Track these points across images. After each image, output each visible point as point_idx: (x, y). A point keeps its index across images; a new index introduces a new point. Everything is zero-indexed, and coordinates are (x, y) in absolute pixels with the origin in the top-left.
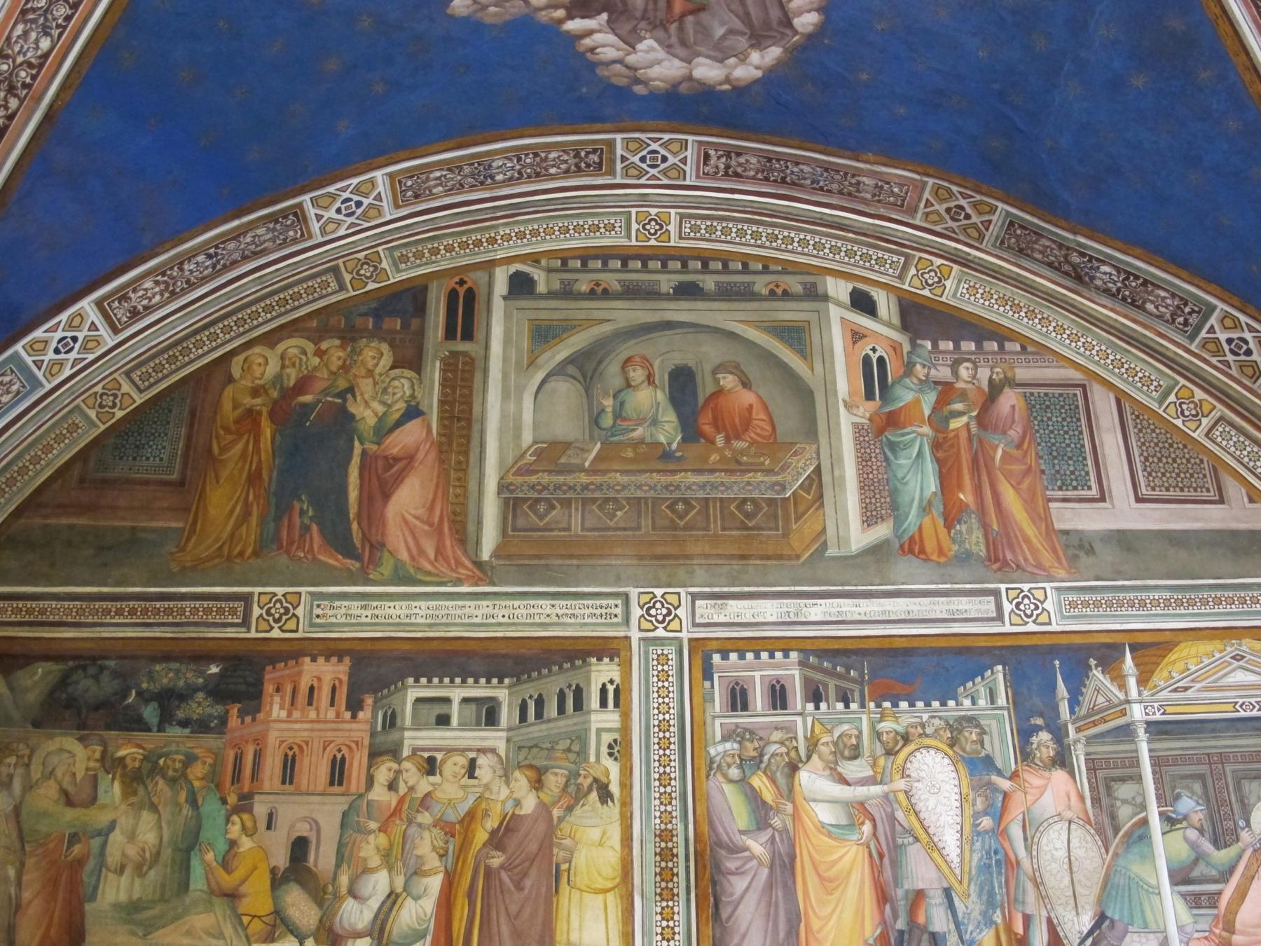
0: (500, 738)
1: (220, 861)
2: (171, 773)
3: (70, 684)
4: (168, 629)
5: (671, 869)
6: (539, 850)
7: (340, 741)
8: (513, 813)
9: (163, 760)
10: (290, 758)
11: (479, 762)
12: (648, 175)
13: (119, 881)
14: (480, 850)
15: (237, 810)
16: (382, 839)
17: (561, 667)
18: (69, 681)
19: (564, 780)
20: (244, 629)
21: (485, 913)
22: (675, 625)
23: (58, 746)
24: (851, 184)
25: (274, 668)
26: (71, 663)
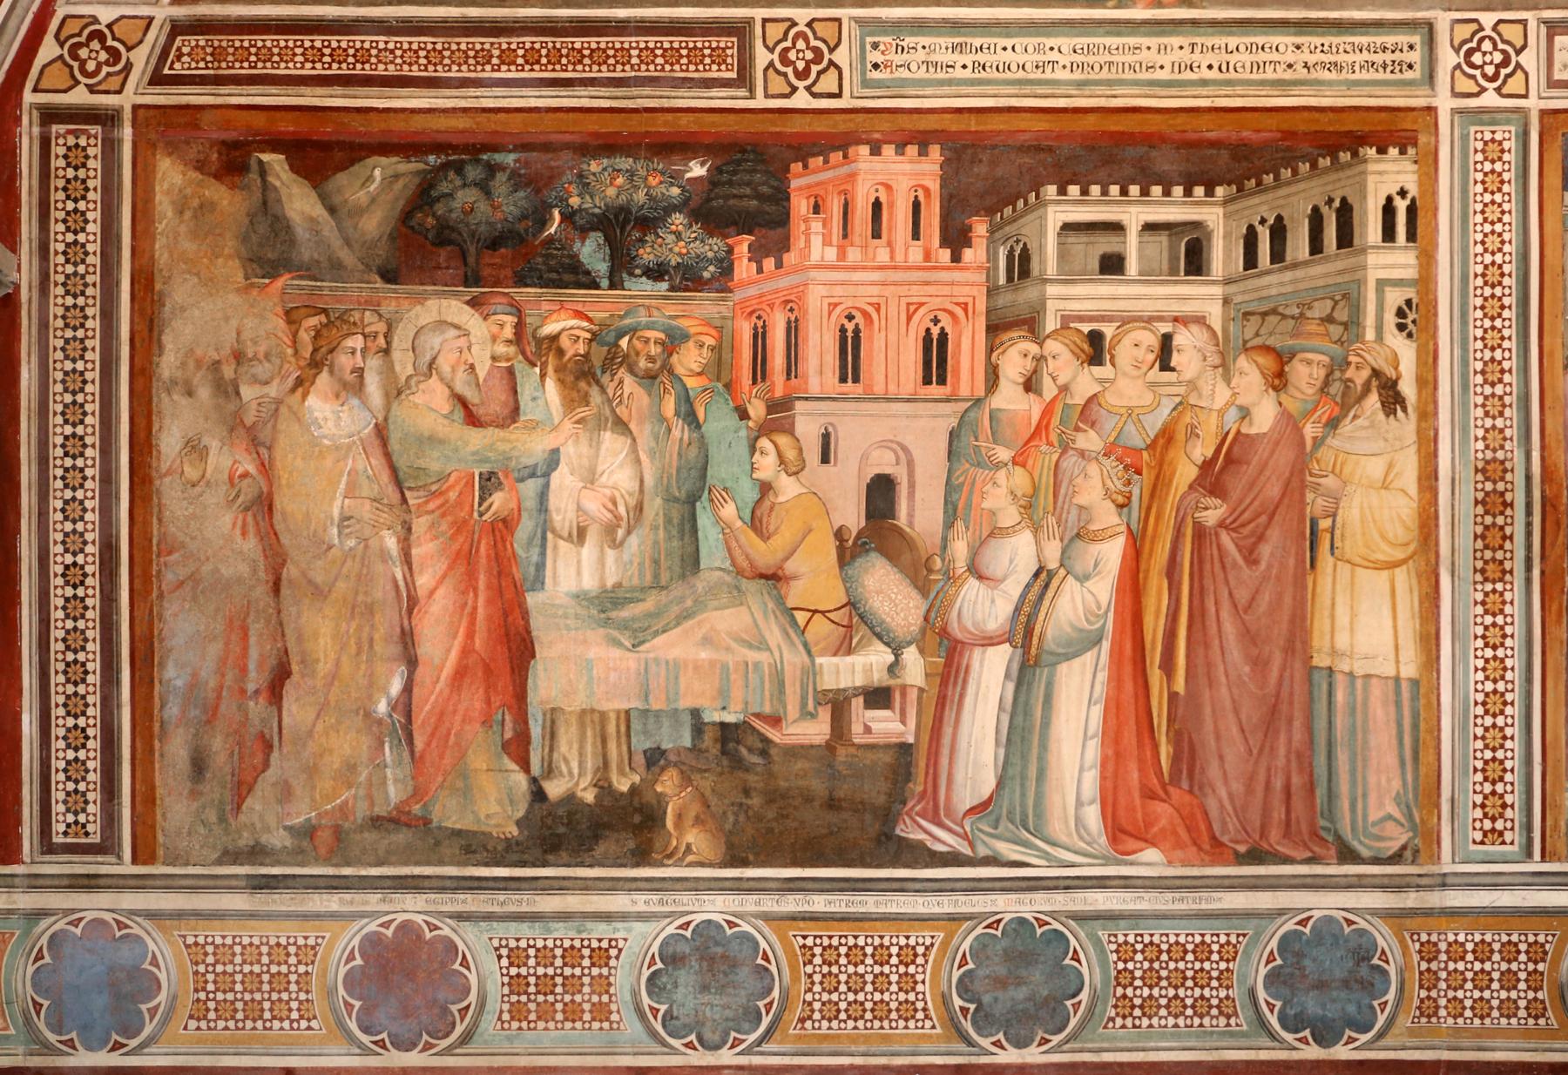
0: (1212, 298)
1: (747, 517)
2: (643, 363)
3: (438, 199)
4: (603, 91)
5: (1502, 528)
6: (1283, 495)
7: (936, 303)
8: (1238, 432)
9: (626, 339)
10: (850, 334)
11: (1178, 340)
13: (579, 554)
14: (1183, 497)
15: (766, 429)
16: (1020, 478)
17: (1314, 166)
19: (1323, 373)
20: (743, 92)
21: (1196, 602)
22: (1516, 85)
23: (434, 316)
25: (805, 166)
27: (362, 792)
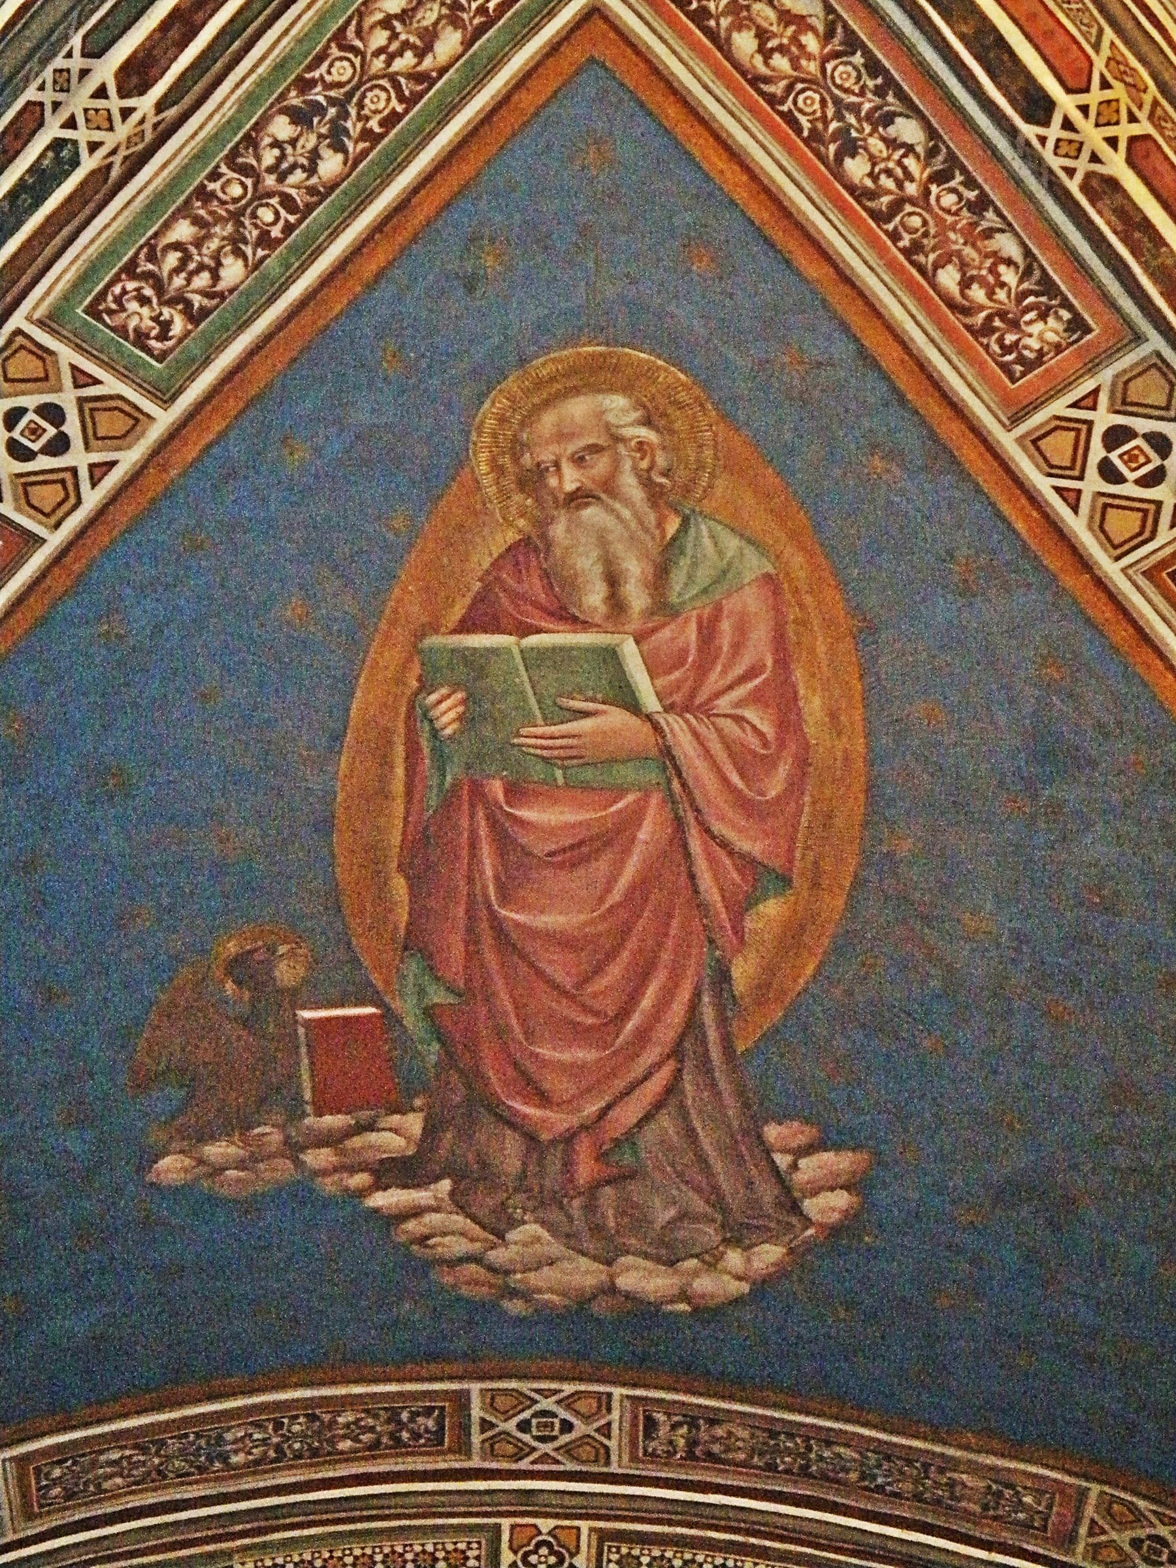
12: (535, 1455)
24: (937, 1485)
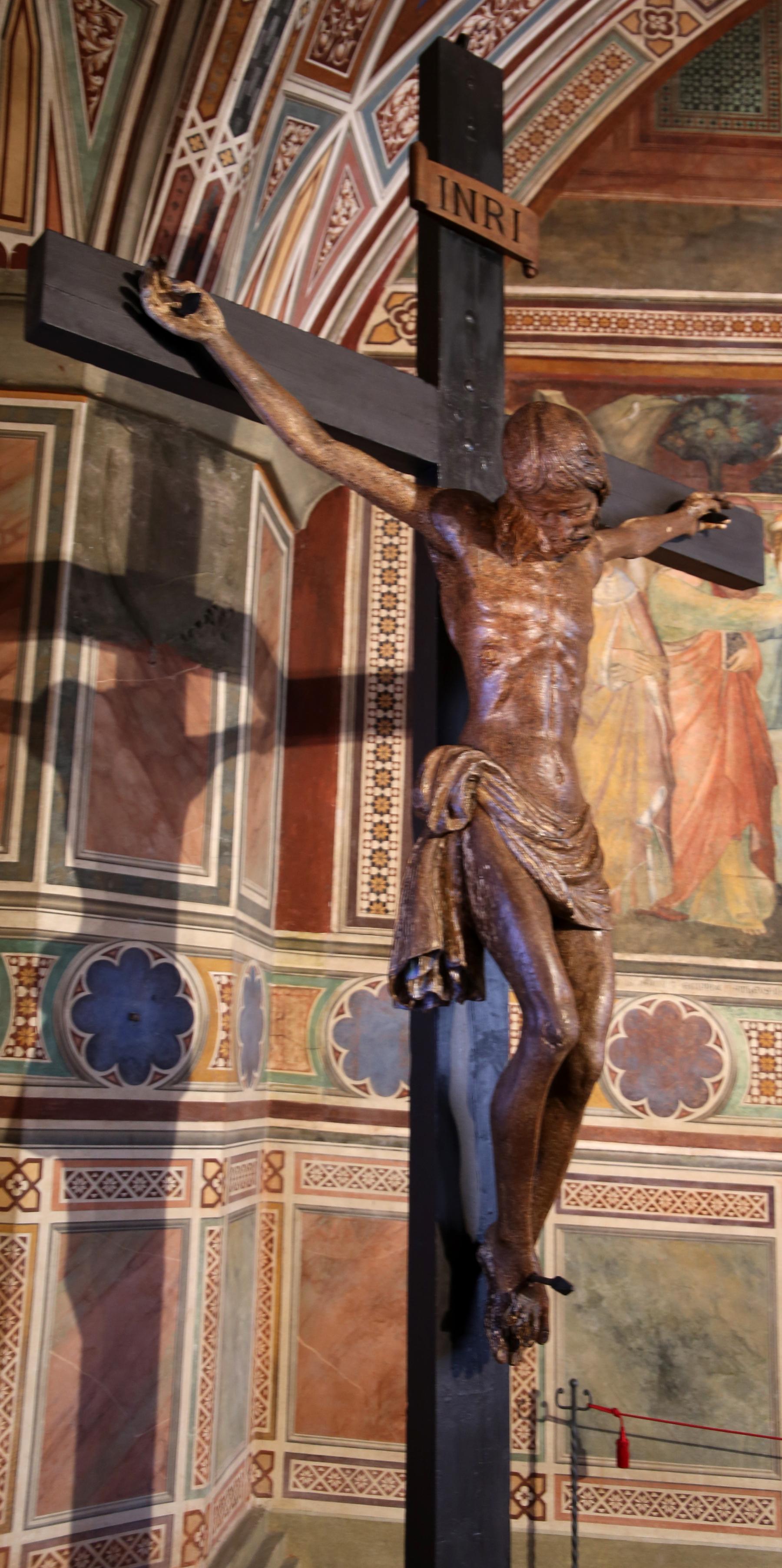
3: (685, 426)
18: (683, 422)
26: (680, 397)
27: (627, 889)
